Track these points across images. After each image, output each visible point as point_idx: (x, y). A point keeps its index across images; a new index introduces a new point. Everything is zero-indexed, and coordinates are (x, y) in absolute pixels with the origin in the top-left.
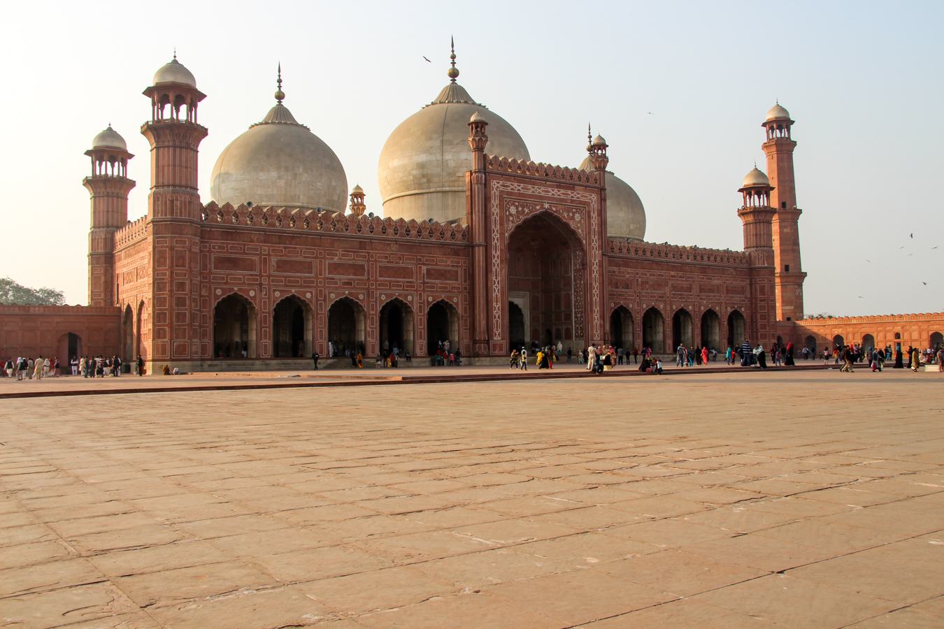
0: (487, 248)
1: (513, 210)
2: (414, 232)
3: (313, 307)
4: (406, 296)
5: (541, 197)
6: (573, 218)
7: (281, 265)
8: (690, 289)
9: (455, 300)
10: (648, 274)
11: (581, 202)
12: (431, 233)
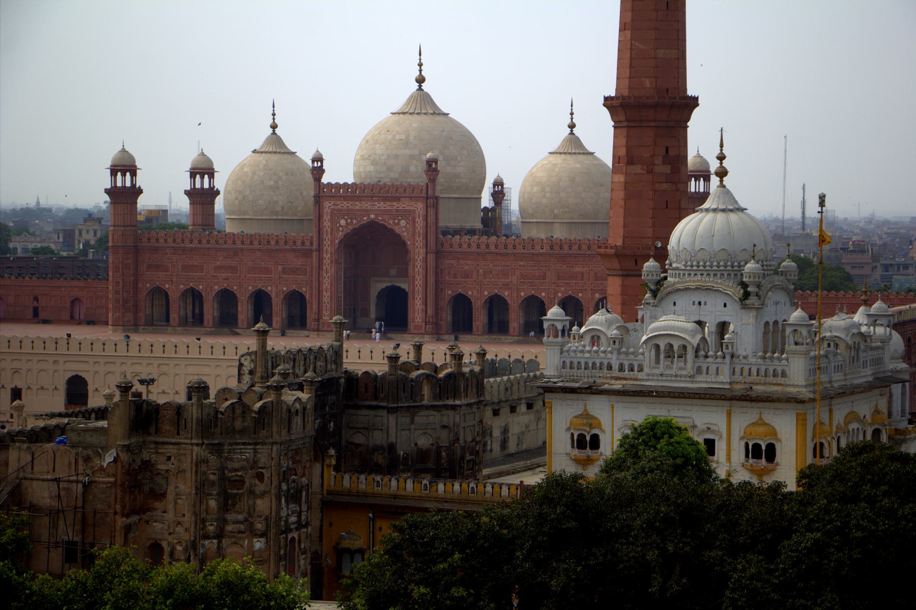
0: (319, 250)
1: (343, 222)
2: (273, 242)
3: (204, 295)
4: (267, 287)
5: (367, 210)
6: (398, 224)
7: (185, 268)
8: (544, 277)
9: (304, 289)
10: (491, 265)
11: (405, 211)
12: (286, 243)
